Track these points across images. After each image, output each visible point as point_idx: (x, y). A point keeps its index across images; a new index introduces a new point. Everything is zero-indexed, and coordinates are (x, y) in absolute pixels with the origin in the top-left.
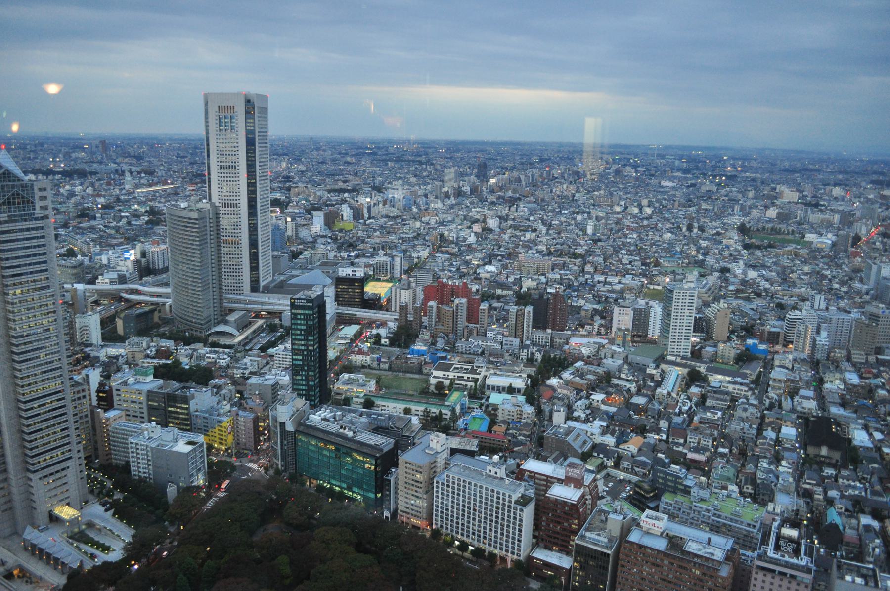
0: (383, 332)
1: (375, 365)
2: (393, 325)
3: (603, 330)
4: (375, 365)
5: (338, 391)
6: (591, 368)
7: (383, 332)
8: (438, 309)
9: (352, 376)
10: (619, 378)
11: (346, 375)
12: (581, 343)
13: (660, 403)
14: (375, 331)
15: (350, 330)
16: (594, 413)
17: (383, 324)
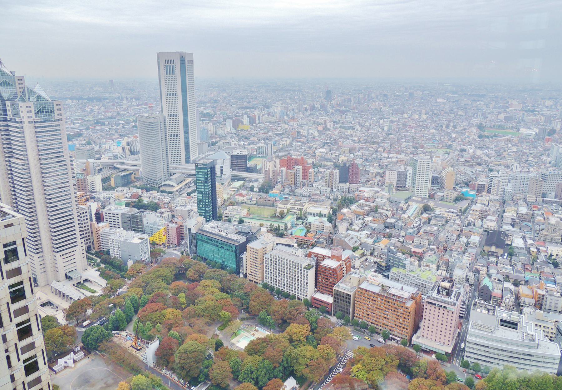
0: (256, 185)
1: (249, 202)
2: (261, 181)
3: (380, 184)
4: (249, 202)
5: (226, 215)
6: (368, 203)
7: (256, 185)
8: (286, 172)
9: (234, 207)
10: (383, 209)
11: (231, 207)
12: (367, 191)
13: (403, 222)
14: (251, 184)
15: (238, 184)
16: (364, 226)
17: (256, 180)
